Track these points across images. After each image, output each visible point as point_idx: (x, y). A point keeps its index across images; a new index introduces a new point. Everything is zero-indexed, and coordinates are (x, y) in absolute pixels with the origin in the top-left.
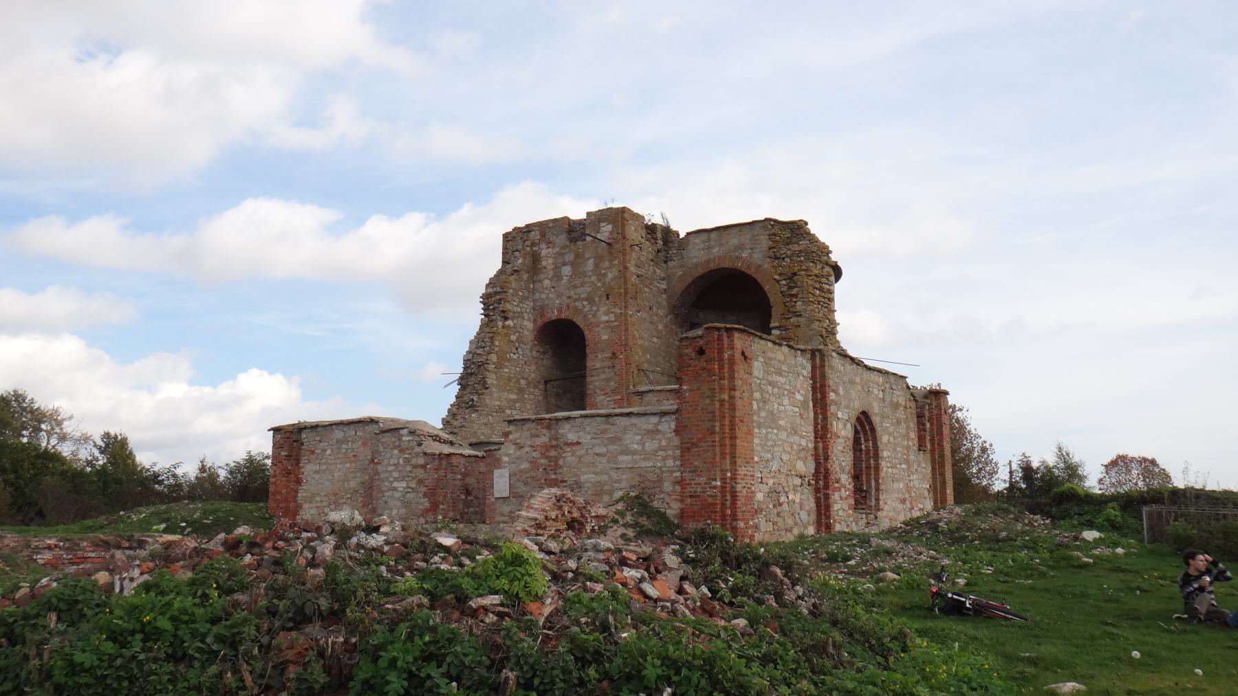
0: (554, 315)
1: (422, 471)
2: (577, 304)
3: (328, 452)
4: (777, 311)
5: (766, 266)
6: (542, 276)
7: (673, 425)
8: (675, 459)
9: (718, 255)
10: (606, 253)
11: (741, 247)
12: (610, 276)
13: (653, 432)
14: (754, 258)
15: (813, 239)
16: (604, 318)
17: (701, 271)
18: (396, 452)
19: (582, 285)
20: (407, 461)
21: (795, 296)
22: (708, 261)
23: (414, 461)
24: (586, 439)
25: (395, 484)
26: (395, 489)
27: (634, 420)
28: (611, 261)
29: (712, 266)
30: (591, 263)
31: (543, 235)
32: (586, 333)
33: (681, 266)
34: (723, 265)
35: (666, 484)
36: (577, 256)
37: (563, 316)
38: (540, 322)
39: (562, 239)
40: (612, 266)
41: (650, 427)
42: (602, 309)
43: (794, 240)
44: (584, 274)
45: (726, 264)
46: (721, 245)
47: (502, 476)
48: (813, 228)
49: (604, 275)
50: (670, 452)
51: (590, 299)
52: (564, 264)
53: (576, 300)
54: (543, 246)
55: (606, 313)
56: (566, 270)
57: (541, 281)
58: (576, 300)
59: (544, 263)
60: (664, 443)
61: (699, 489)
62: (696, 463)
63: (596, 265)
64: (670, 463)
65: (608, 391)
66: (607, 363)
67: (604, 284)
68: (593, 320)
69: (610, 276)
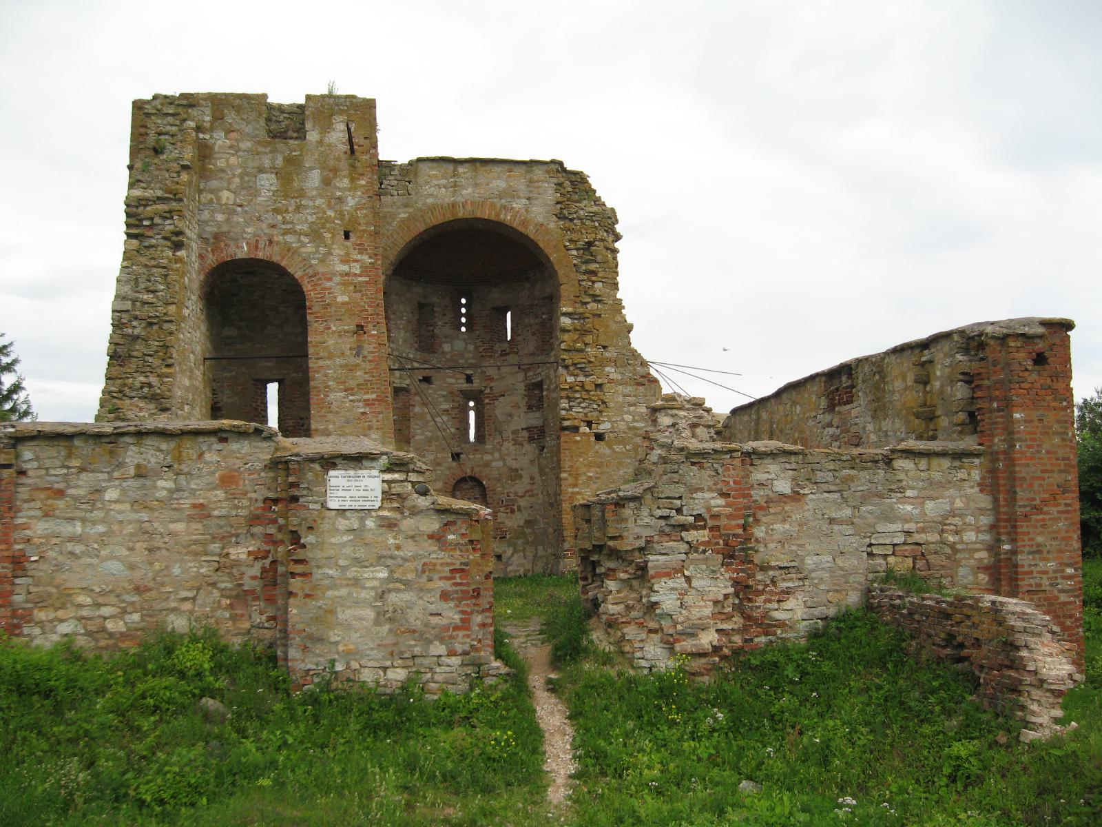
0: (243, 251)
2: (289, 238)
3: (112, 494)
4: (567, 290)
5: (552, 225)
6: (214, 184)
7: (976, 475)
8: (978, 530)
9: (470, 198)
10: (344, 165)
11: (512, 193)
12: (351, 202)
14: (533, 213)
15: (597, 201)
16: (345, 268)
17: (437, 219)
21: (594, 273)
22: (454, 205)
26: (356, 582)
28: (352, 180)
29: (461, 214)
30: (314, 179)
31: (218, 117)
32: (307, 287)
33: (406, 206)
34: (479, 215)
35: (961, 571)
36: (289, 161)
37: (260, 255)
38: (212, 260)
39: (259, 127)
40: (354, 188)
42: (338, 251)
43: (576, 197)
44: (302, 193)
45: (486, 214)
46: (476, 185)
48: (594, 183)
49: (340, 200)
50: (970, 519)
51: (315, 234)
52: (261, 170)
54: (219, 134)
55: (345, 261)
56: (267, 183)
57: (214, 191)
58: (286, 232)
59: (221, 164)
60: (959, 503)
61: (1045, 582)
62: (1040, 539)
63: (327, 182)
64: (970, 536)
67: (342, 217)
68: (321, 269)
69: (351, 202)
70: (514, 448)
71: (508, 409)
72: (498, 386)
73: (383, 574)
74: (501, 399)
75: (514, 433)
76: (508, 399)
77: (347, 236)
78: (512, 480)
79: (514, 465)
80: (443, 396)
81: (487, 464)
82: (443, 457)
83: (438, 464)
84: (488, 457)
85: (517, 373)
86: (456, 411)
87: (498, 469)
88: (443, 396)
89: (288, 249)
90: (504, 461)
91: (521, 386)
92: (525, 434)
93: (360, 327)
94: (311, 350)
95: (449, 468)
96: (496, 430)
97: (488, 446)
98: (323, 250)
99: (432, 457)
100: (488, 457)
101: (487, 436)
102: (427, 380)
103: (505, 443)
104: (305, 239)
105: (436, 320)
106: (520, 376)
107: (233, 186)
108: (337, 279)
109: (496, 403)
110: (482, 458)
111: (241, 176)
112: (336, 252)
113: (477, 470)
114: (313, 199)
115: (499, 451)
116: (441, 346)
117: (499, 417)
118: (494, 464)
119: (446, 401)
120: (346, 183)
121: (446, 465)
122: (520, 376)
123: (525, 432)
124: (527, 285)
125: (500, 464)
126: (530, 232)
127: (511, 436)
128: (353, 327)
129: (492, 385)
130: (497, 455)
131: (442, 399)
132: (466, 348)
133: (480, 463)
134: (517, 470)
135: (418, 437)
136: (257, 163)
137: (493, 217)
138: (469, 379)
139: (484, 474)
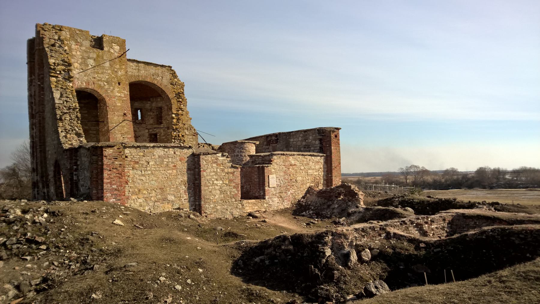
1: (231, 175)
2: (100, 83)
13: (318, 162)
14: (162, 81)
18: (214, 165)
19: (102, 73)
20: (223, 170)
23: (226, 170)
24: (298, 163)
25: (215, 182)
27: (313, 158)
28: (120, 66)
30: (107, 64)
32: (107, 99)
34: (146, 80)
36: (98, 56)
41: (318, 160)
47: (273, 178)
53: (99, 80)
56: (91, 62)
58: (99, 80)
65: (123, 132)
66: (121, 119)
73: (221, 182)
77: (119, 84)
89: (100, 86)
91: (147, 135)
93: (125, 114)
94: (109, 120)
98: (112, 88)
104: (106, 84)
106: (147, 131)
107: (79, 62)
108: (117, 98)
111: (81, 59)
112: (116, 89)
114: (107, 70)
120: (118, 66)
122: (147, 131)
124: (149, 102)
126: (163, 87)
128: (122, 114)
136: (87, 55)
137: (151, 82)
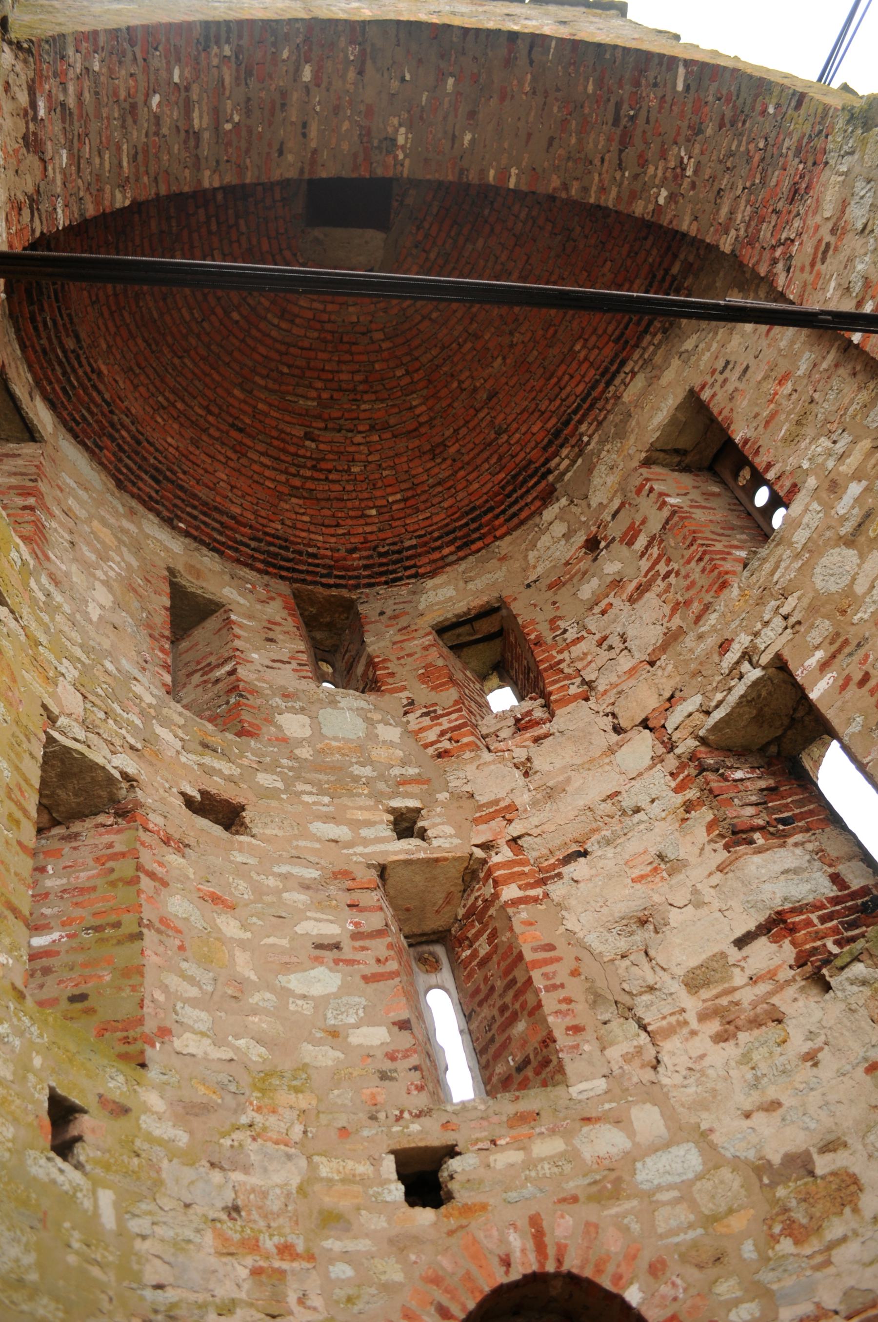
70: (730, 1050)
71: (627, 898)
72: (546, 827)
74: (579, 868)
75: (694, 982)
76: (604, 859)
78: (797, 1233)
79: (776, 1139)
80: (306, 886)
81: (611, 1184)
82: (349, 1180)
83: (332, 1220)
84: (606, 1142)
85: (611, 750)
86: (379, 947)
87: (685, 1193)
88: (306, 886)
90: (703, 1138)
91: (659, 781)
92: (766, 954)
95: (400, 1244)
96: (596, 999)
97: (585, 1085)
99: (285, 1175)
100: (606, 1142)
101: (563, 1040)
102: (227, 815)
103: (670, 1047)
105: (237, 643)
109: (557, 890)
110: (572, 1156)
113: (563, 1227)
115: (653, 1093)
116: (269, 721)
117: (592, 940)
118: (651, 1172)
119: (320, 906)
121: (377, 1223)
123: (762, 946)
125: (686, 1160)
127: (692, 1004)
129: (515, 829)
130: (648, 1120)
131: (300, 898)
132: (372, 736)
133: (572, 1186)
134: (800, 1164)
135: (187, 1043)
138: (406, 825)
139: (613, 1243)
